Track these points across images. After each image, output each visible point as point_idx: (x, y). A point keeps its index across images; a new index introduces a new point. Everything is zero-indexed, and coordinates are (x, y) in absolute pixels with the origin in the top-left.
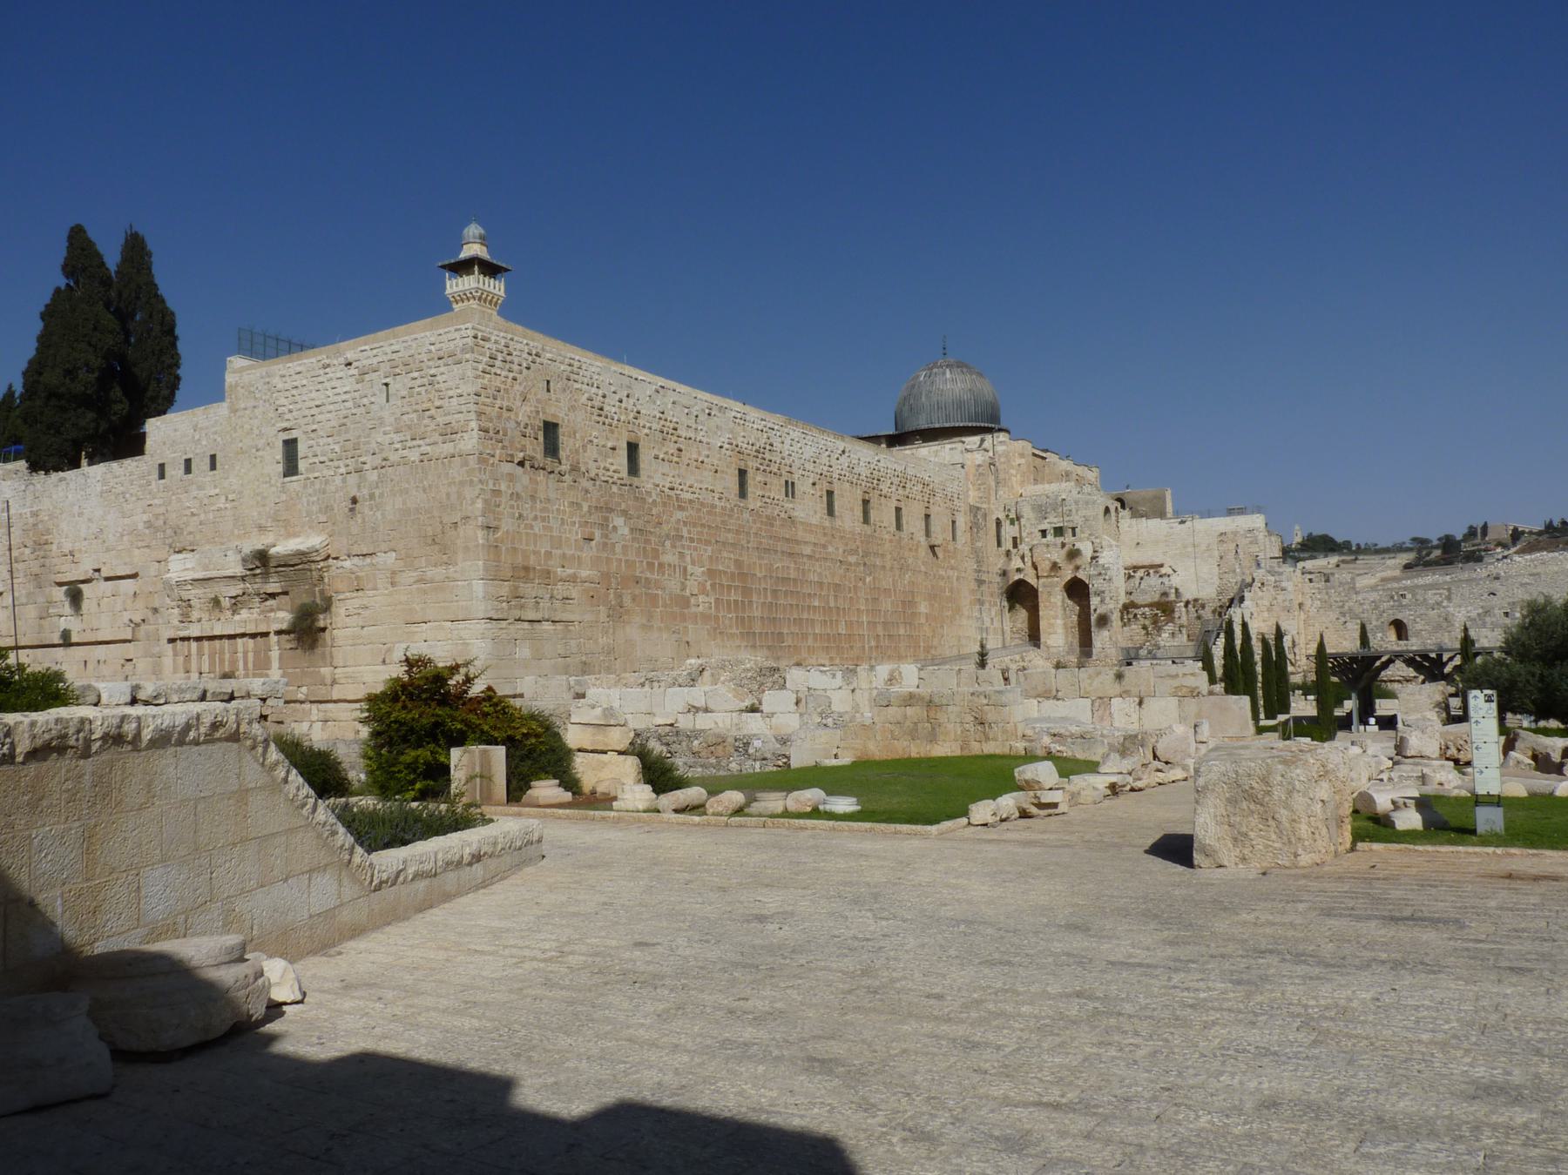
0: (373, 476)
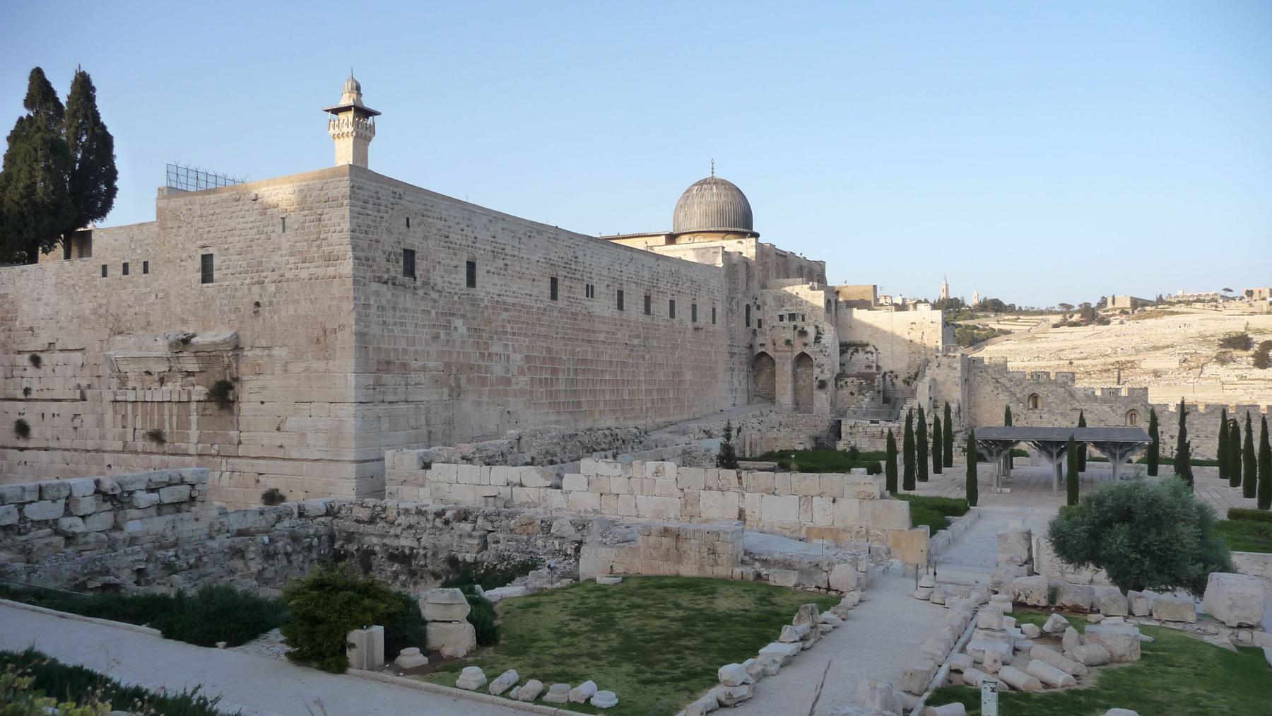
0: (272, 288)
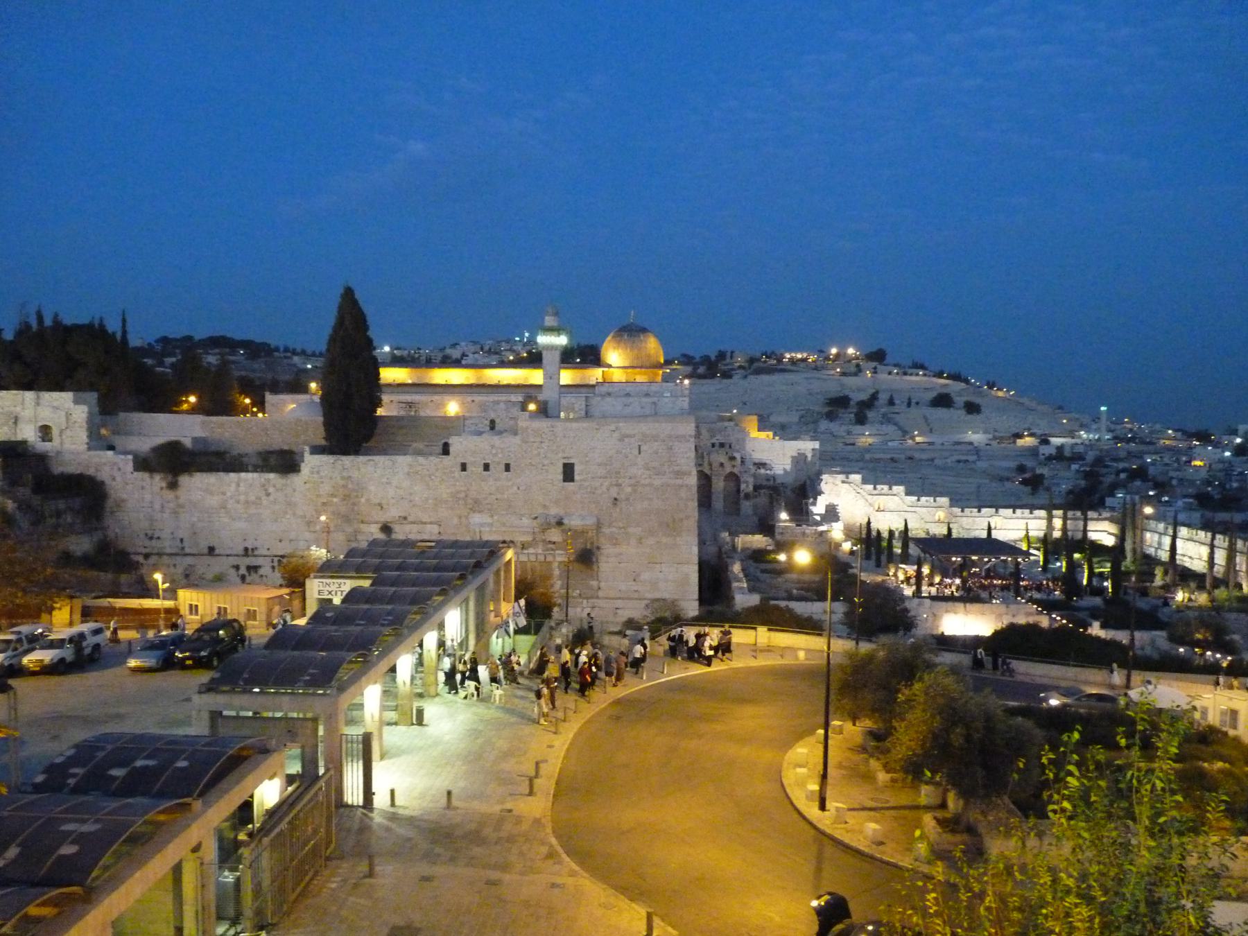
0: (629, 490)
